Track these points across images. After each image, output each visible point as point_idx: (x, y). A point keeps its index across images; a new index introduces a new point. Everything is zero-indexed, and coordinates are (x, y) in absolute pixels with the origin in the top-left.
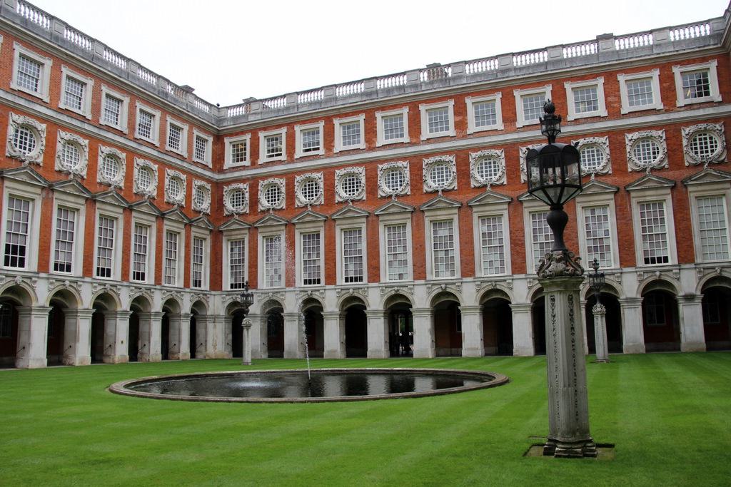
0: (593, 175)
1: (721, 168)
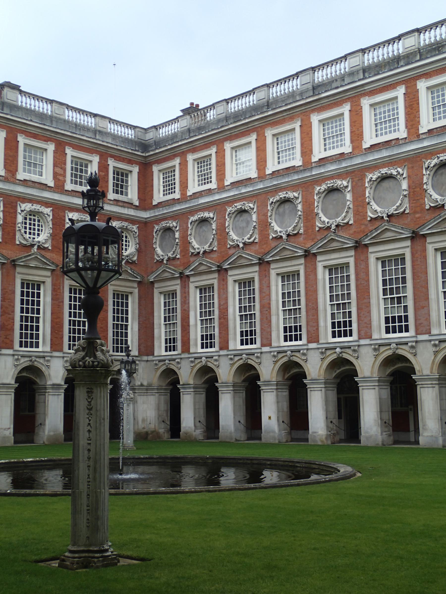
0: (36, 247)
1: (133, 267)
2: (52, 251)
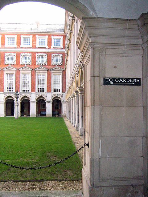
1: (61, 67)
2: (32, 65)
